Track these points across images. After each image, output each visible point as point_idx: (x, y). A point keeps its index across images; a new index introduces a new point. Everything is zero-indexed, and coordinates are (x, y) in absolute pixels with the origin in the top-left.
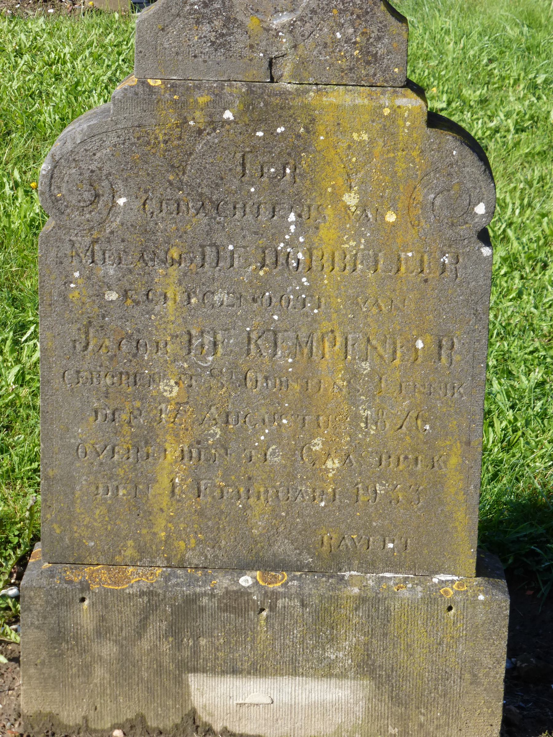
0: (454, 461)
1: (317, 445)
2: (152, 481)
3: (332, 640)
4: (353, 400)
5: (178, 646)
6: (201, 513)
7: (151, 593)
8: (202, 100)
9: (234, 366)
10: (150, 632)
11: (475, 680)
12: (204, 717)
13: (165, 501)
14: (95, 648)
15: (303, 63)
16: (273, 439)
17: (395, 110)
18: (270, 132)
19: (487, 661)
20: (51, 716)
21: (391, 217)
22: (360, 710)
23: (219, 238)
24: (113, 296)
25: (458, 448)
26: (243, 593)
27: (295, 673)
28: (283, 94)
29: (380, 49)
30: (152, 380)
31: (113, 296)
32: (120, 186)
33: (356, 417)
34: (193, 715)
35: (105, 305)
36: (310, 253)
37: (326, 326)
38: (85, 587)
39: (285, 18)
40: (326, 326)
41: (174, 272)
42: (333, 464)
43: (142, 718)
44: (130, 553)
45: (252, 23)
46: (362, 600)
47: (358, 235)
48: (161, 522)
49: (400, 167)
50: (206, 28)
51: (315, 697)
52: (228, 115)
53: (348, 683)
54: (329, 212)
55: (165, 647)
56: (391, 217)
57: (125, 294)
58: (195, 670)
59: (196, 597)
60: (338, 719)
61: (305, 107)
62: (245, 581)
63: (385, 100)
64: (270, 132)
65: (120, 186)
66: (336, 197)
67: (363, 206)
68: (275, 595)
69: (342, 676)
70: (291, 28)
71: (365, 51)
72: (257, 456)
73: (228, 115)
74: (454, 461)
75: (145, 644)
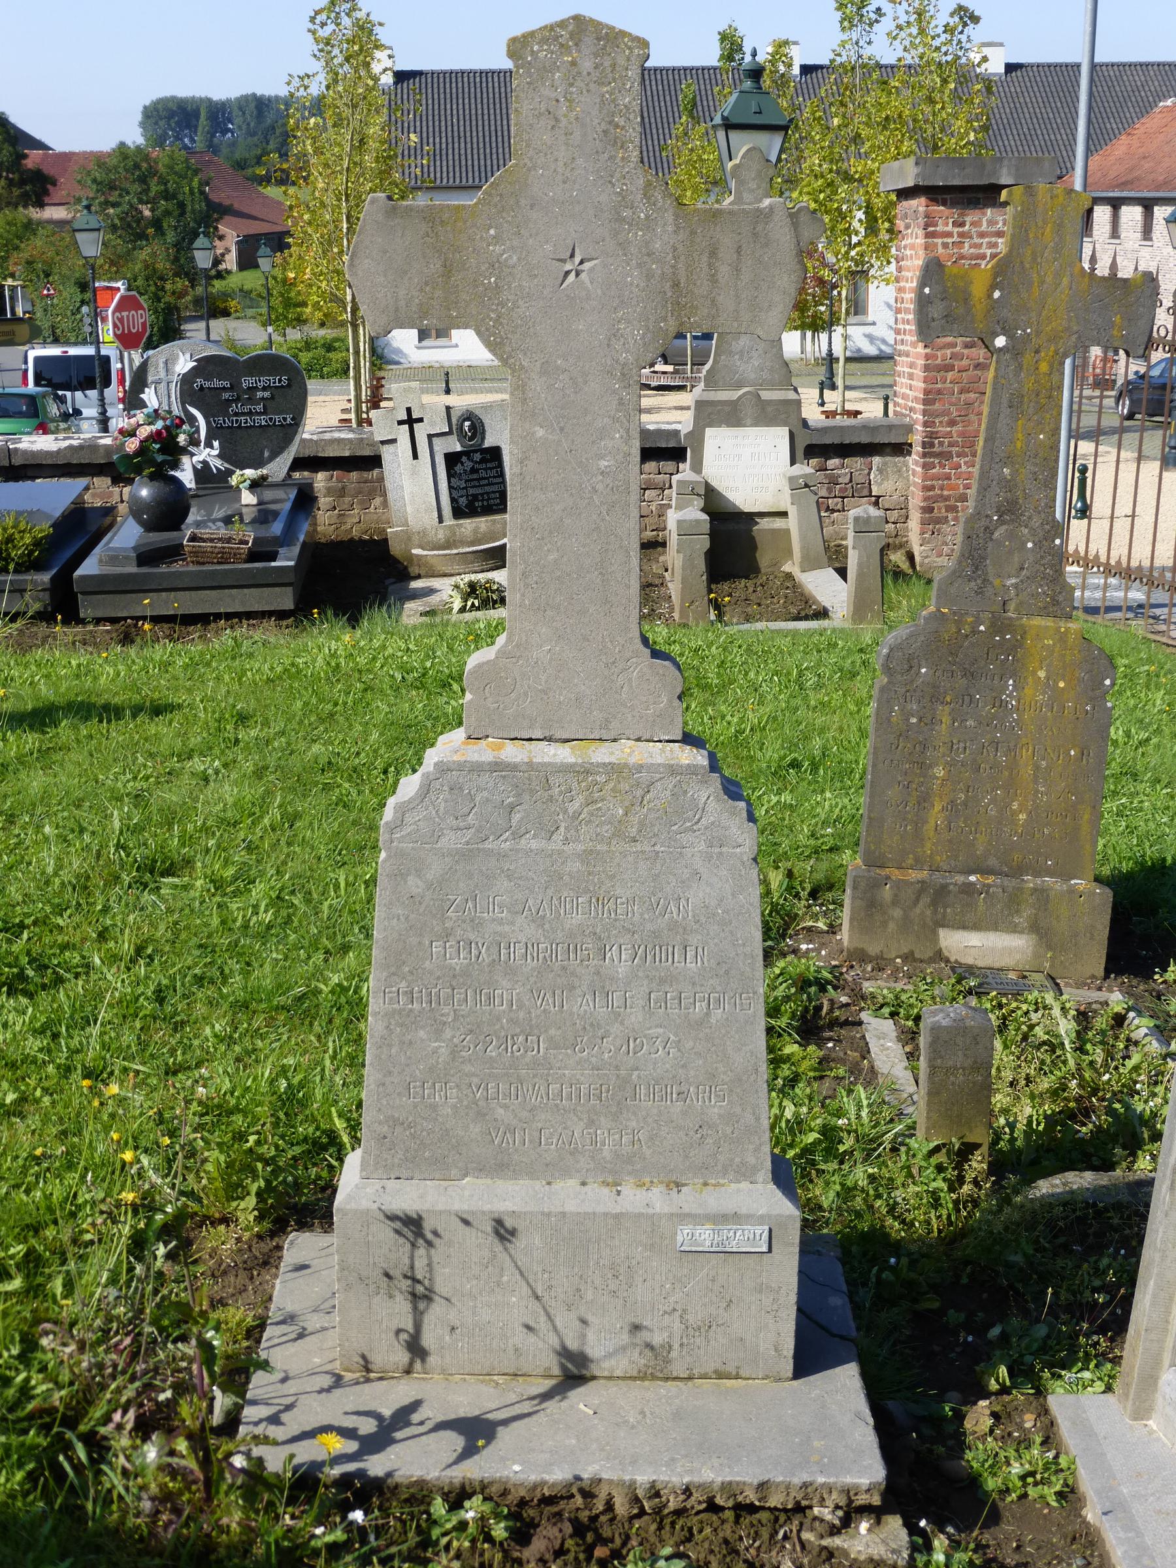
0: (1086, 817)
1: (1015, 806)
2: (926, 822)
3: (1017, 911)
4: (1036, 781)
5: (935, 912)
6: (950, 841)
7: (923, 882)
8: (970, 619)
9: (975, 760)
10: (921, 905)
11: (1092, 938)
12: (946, 954)
13: (932, 833)
14: (890, 912)
15: (1021, 603)
16: (991, 802)
17: (1067, 629)
18: (1003, 638)
19: (1100, 927)
20: (863, 950)
21: (1062, 684)
22: (1029, 951)
23: (972, 691)
24: (914, 720)
25: (1089, 810)
26: (972, 884)
27: (996, 929)
28: (1010, 618)
29: (1061, 599)
30: (931, 766)
31: (914, 720)
32: (923, 663)
33: (1037, 791)
34: (940, 952)
35: (910, 725)
36: (1018, 702)
37: (1024, 741)
38: (888, 878)
39: (1013, 581)
40: (1024, 741)
41: (947, 708)
42: (1022, 816)
43: (912, 953)
44: (910, 861)
45: (997, 582)
46: (1035, 890)
47: (1044, 693)
48: (928, 845)
49: (1068, 659)
50: (973, 584)
51: (1006, 943)
52: (982, 628)
53: (1025, 936)
54: (1030, 679)
55: (928, 912)
56: (1062, 684)
57: (920, 720)
58: (943, 926)
59: (947, 885)
60: (1018, 957)
61: (1022, 625)
62: (972, 878)
63: (1062, 624)
64: (1003, 638)
65: (923, 663)
66: (1034, 673)
67: (1048, 678)
68: (989, 886)
69: (1021, 932)
70: (1016, 586)
71: (1053, 599)
72: (982, 810)
73: (982, 628)
74: (1086, 817)
75: (918, 911)
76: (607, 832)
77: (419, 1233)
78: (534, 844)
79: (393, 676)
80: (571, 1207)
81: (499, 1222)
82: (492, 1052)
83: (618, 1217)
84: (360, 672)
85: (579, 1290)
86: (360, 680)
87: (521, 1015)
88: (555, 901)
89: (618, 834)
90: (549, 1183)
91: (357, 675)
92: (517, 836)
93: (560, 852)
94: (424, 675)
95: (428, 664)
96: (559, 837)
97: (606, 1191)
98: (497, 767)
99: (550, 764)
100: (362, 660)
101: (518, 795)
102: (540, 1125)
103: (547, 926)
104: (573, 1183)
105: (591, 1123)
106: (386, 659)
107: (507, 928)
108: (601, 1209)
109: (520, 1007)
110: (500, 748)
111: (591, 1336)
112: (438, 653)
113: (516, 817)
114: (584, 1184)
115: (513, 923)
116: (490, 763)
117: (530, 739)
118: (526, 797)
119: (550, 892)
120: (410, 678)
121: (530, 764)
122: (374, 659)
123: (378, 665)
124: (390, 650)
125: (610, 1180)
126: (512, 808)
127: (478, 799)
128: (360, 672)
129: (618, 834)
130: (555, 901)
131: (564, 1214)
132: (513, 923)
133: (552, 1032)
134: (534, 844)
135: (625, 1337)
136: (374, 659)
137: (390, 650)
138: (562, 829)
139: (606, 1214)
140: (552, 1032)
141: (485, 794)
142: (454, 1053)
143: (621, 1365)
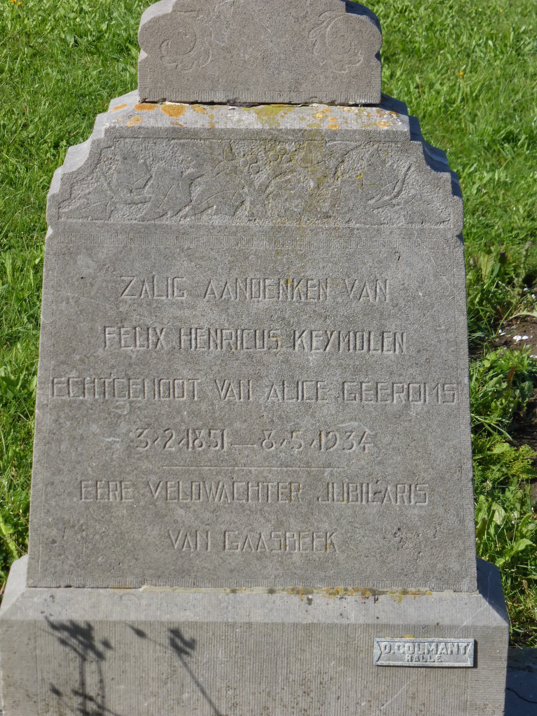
76: (296, 205)
77: (89, 644)
78: (217, 221)
79: (64, 40)
81: (176, 633)
82: (172, 447)
83: (308, 627)
84: (28, 35)
85: (266, 708)
86: (28, 44)
87: (204, 407)
88: (240, 284)
89: (309, 209)
90: (234, 591)
91: (24, 39)
92: (198, 211)
93: (245, 230)
94: (99, 39)
95: (104, 27)
96: (244, 212)
97: (295, 599)
99: (233, 130)
100: (30, 23)
101: (199, 166)
102: (224, 527)
103: (231, 311)
104: (260, 591)
105: (280, 524)
106: (57, 21)
107: (187, 313)
108: (291, 619)
109: (202, 399)
110: (179, 112)
112: (115, 14)
113: (197, 190)
114: (271, 591)
115: (194, 307)
116: (167, 130)
117: (212, 103)
118: (208, 167)
119: (235, 273)
120: (83, 42)
121: (212, 132)
122: (44, 21)
123: (48, 27)
124: (62, 12)
125: (300, 587)
126: (192, 180)
127: (154, 170)
128: (28, 35)
129: (309, 209)
130: (240, 284)
131: (250, 625)
132: (194, 307)
133: (237, 425)
134: (217, 221)
136: (44, 21)
137: (62, 12)
138: (247, 204)
139: (295, 625)
140: (237, 425)
141: (162, 164)
142: (130, 449)
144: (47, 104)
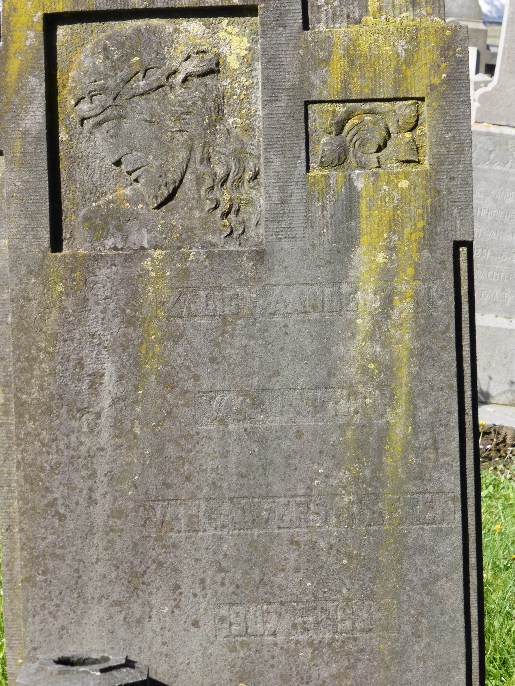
78: (498, 168)
80: (492, 325)
83: (511, 330)
85: (489, 362)
87: (482, 240)
88: (503, 193)
90: (482, 315)
92: (492, 163)
93: (508, 172)
96: (508, 165)
97: (506, 320)
98: (488, 134)
99: (508, 135)
101: (495, 147)
102: (482, 289)
103: (498, 203)
104: (492, 316)
105: (503, 290)
107: (482, 202)
108: (504, 326)
109: (482, 236)
110: (489, 127)
111: (492, 383)
113: (492, 156)
114: (497, 316)
115: (484, 200)
116: (485, 132)
117: (500, 125)
118: (498, 148)
119: (502, 188)
121: (501, 135)
125: (508, 316)
126: (491, 152)
127: (478, 147)
130: (503, 193)
131: (488, 327)
132: (484, 200)
133: (493, 248)
134: (498, 168)
135: (506, 387)
138: (510, 163)
139: (505, 329)
140: (493, 248)
141: (481, 145)
143: (503, 399)
144: (254, 248)
